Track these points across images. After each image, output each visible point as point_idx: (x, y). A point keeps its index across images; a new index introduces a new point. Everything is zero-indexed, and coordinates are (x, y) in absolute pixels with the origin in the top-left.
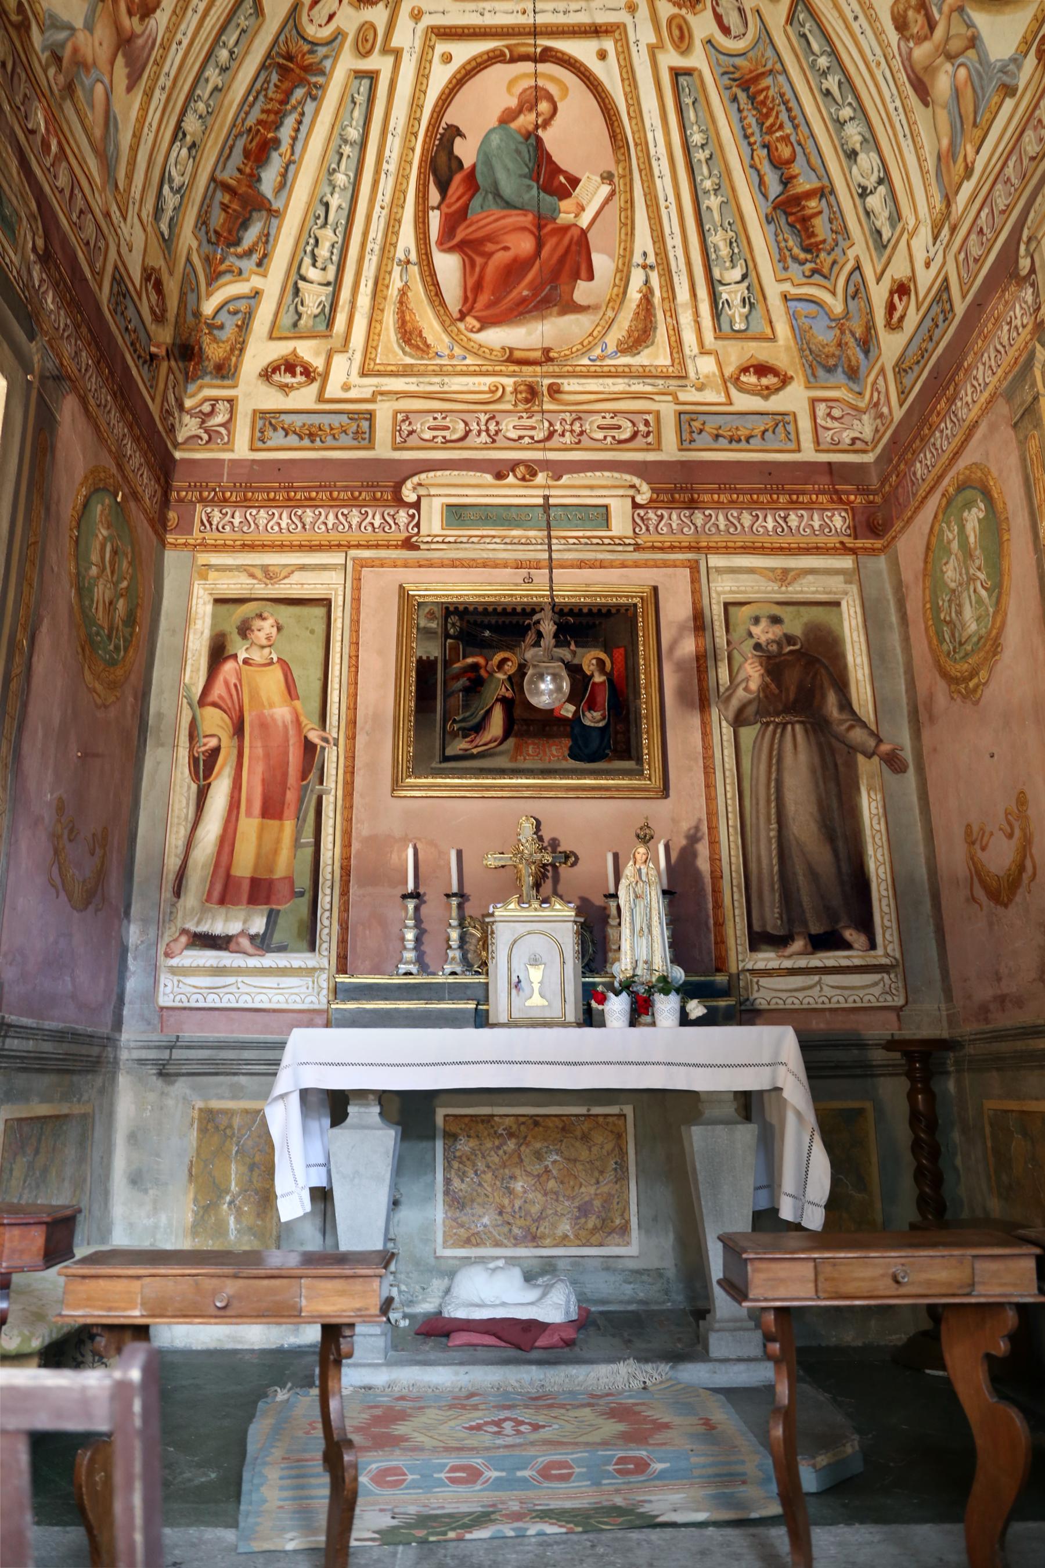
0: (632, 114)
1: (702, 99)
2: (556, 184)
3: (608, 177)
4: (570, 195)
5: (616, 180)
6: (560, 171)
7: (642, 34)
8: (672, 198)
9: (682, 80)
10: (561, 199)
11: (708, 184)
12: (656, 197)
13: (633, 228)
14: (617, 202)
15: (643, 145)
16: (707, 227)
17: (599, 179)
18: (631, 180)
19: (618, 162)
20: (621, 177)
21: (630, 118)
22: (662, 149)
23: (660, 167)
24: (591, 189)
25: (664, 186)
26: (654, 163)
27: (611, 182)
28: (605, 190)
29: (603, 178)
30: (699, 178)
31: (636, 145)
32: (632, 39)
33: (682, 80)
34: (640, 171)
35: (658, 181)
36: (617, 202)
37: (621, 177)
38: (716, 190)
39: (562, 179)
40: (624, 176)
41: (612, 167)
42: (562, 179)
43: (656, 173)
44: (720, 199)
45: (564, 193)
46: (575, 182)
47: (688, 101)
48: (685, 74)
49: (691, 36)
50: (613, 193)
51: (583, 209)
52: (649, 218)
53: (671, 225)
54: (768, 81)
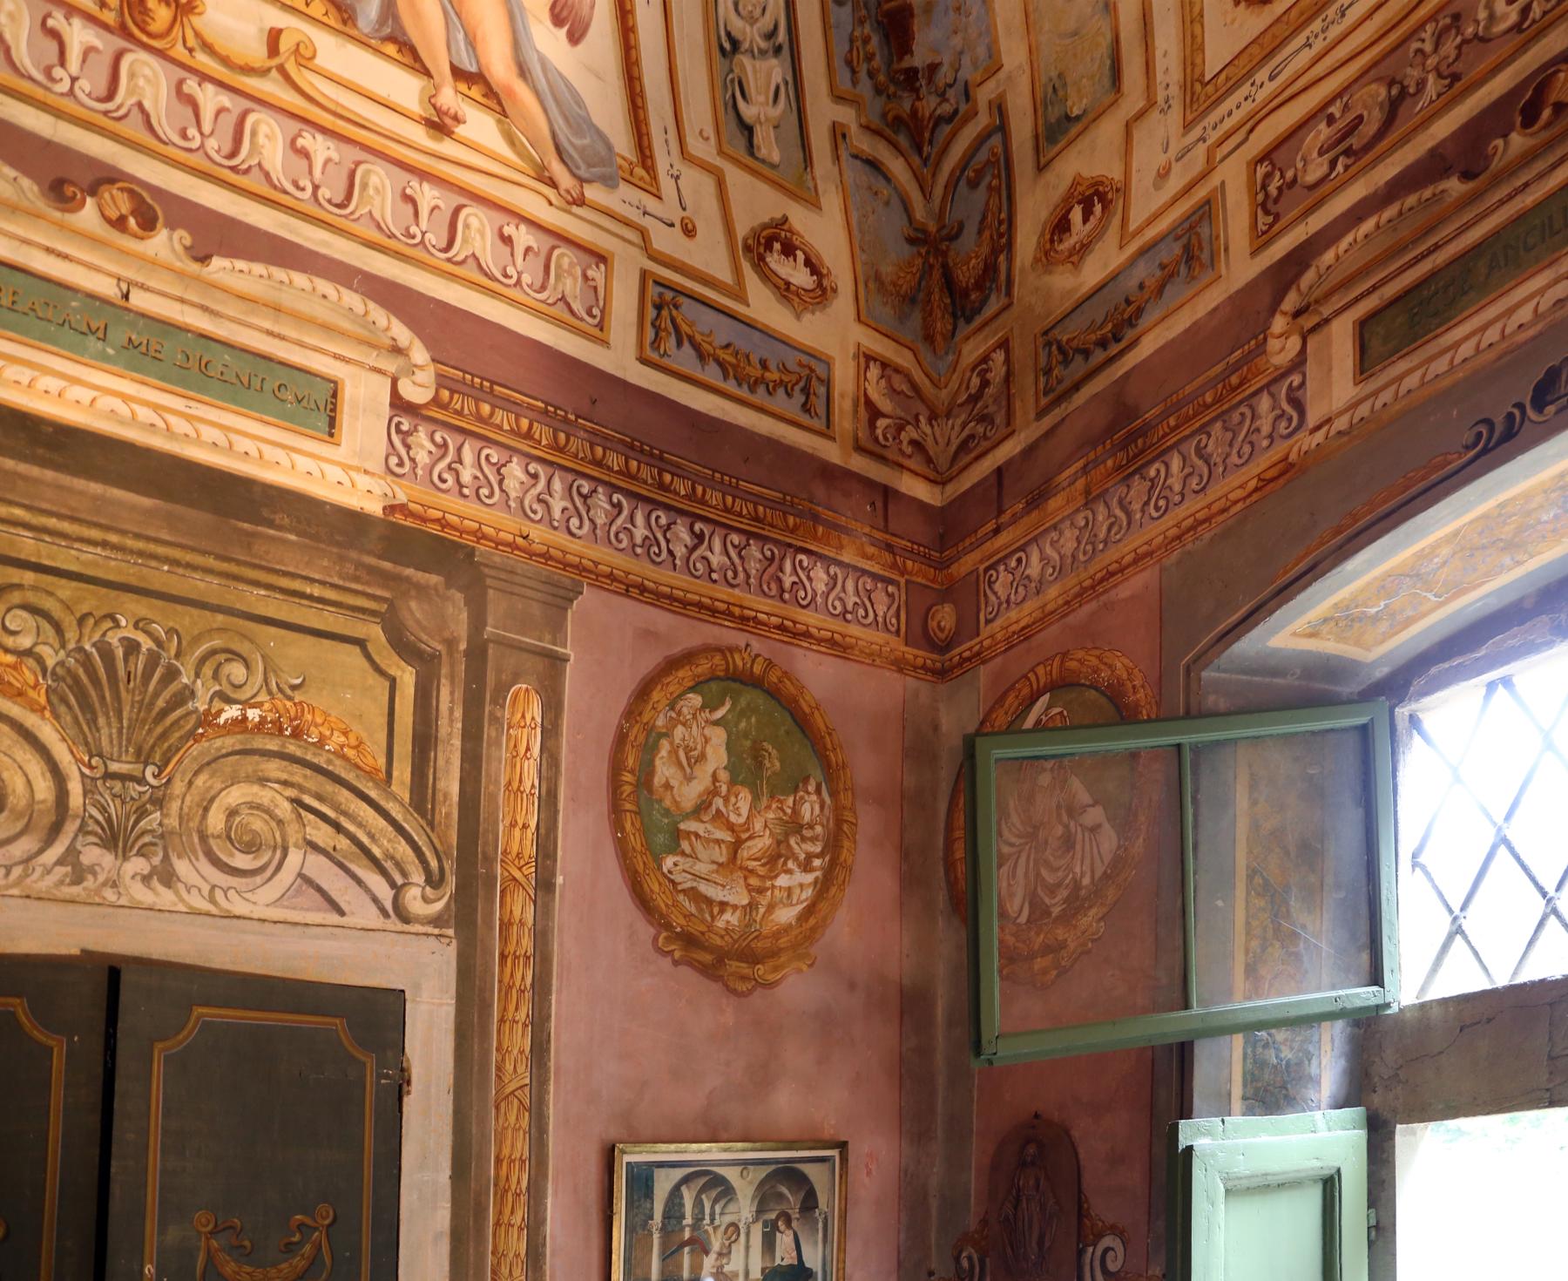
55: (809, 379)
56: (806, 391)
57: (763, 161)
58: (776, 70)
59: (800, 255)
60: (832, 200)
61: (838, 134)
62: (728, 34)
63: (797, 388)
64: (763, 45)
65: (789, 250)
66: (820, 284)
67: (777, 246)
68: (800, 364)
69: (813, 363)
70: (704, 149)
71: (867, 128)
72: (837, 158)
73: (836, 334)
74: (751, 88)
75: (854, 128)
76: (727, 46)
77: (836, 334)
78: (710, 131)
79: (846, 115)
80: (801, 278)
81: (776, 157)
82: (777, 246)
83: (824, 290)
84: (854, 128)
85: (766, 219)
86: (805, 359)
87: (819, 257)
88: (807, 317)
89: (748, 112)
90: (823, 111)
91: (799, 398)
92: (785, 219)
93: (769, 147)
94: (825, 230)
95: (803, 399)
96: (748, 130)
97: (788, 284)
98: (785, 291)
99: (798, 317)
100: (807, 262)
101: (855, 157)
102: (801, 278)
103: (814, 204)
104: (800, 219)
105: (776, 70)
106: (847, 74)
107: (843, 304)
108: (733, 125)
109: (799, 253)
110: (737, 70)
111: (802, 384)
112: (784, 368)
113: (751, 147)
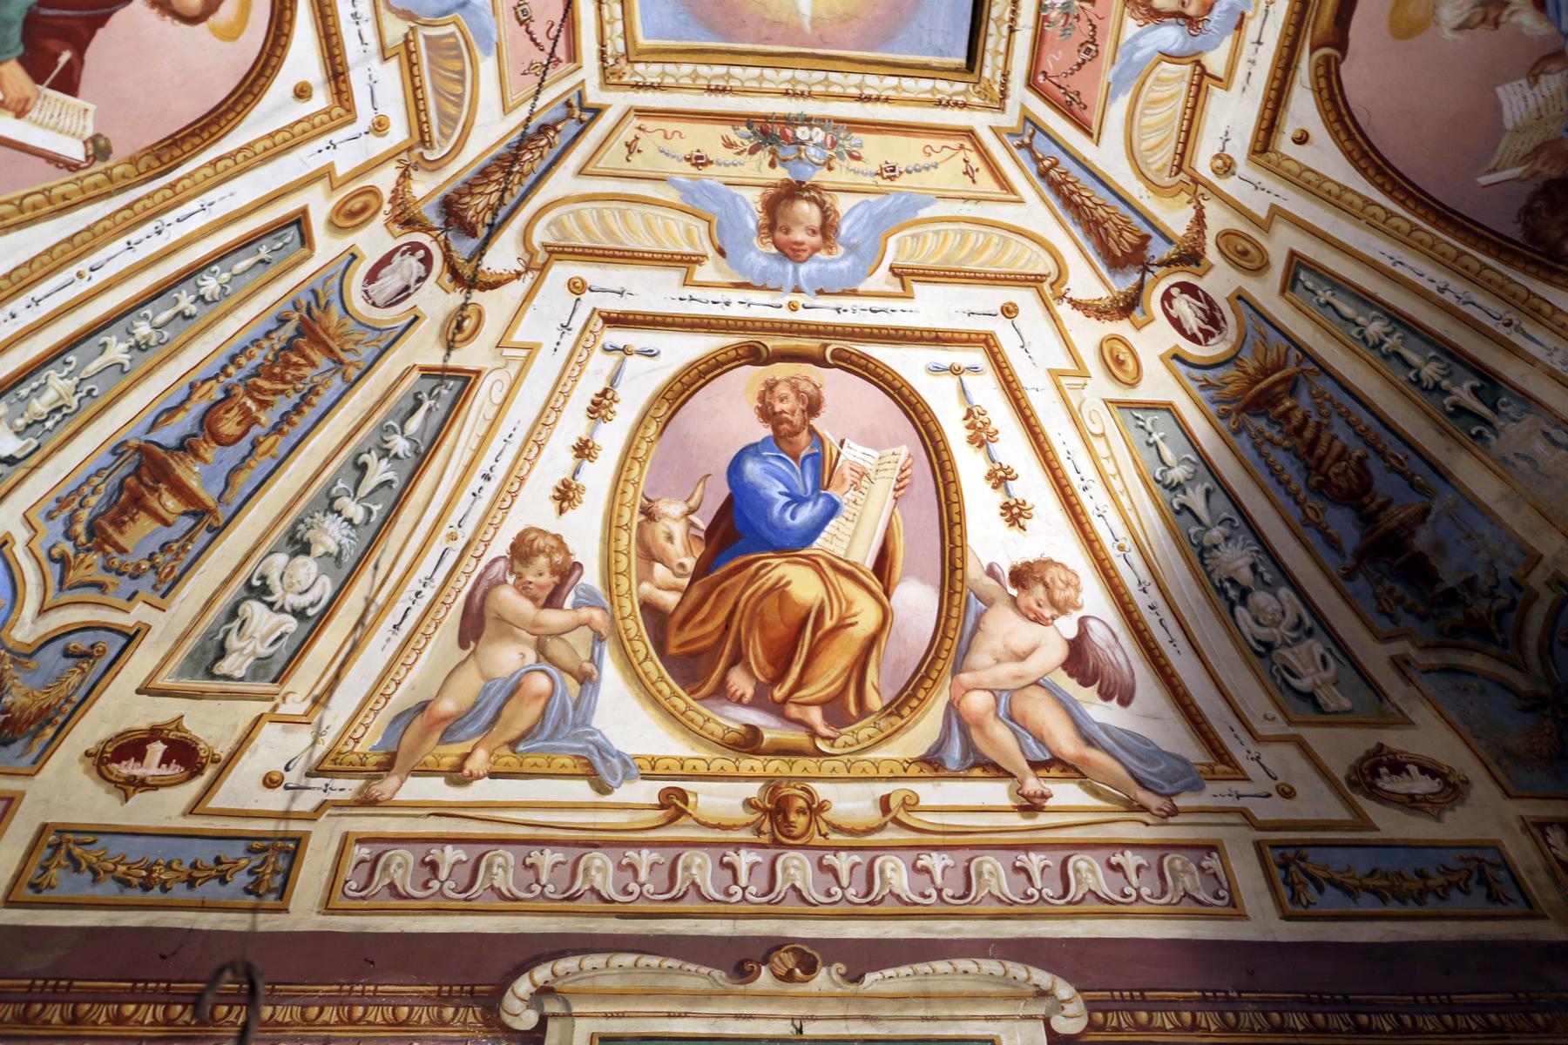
0: (220, 165)
1: (271, 271)
2: (52, 44)
3: (99, 149)
4: (38, 78)
5: (99, 166)
6: (80, 48)
7: (346, 151)
8: (99, 278)
9: (293, 231)
10: (23, 61)
11: (143, 329)
12: (92, 249)
13: (19, 226)
14: (61, 182)
15: (176, 198)
16: (71, 358)
17: (89, 133)
18: (108, 195)
19: (133, 161)
20: (107, 173)
21: (213, 163)
22: (176, 233)
23: (147, 241)
24: (66, 122)
25: (116, 256)
26: (150, 227)
27: (92, 158)
28: (74, 150)
29: (94, 139)
30: (148, 311)
31: (172, 186)
32: (336, 136)
33: (293, 231)
34: (129, 207)
35: (120, 244)
36: (61, 182)
37: (107, 173)
38: (138, 346)
39: (65, 57)
40: (110, 179)
41: (120, 152)
42: (65, 57)
43: (133, 237)
44: (125, 359)
45: (37, 66)
46: (68, 83)
47: (264, 252)
48: (302, 235)
49: (356, 227)
50: (72, 166)
51: (19, 115)
52: (49, 251)
53: (52, 293)
54: (317, 356)
55: (1482, 872)
56: (1483, 881)
57: (1336, 713)
58: (1317, 647)
59: (1412, 768)
60: (1422, 713)
61: (1400, 665)
62: (1259, 642)
63: (1472, 883)
64: (1294, 635)
65: (1398, 768)
66: (1447, 784)
67: (1383, 770)
68: (1462, 859)
69: (1477, 853)
70: (1279, 727)
71: (1427, 647)
72: (1408, 680)
73: (1489, 817)
74: (1298, 666)
75: (1413, 652)
76: (1261, 649)
77: (1489, 817)
78: (1272, 711)
79: (1400, 647)
80: (1423, 785)
81: (1346, 704)
82: (1383, 770)
83: (1454, 786)
84: (1413, 652)
85: (1362, 753)
86: (1466, 853)
87: (1433, 761)
88: (1448, 816)
89: (1303, 684)
90: (1375, 656)
91: (1479, 893)
92: (1381, 746)
93: (1334, 699)
94: (1428, 736)
95: (1484, 890)
96: (1310, 697)
97: (1411, 796)
98: (1411, 803)
99: (1438, 819)
100: (1423, 770)
101: (1427, 672)
102: (1423, 785)
103: (1404, 722)
104: (1394, 740)
105: (1317, 647)
106: (1386, 621)
107: (1483, 789)
108: (1293, 699)
109: (1409, 767)
110: (1279, 662)
111: (1475, 876)
112: (1447, 870)
113: (1318, 707)
